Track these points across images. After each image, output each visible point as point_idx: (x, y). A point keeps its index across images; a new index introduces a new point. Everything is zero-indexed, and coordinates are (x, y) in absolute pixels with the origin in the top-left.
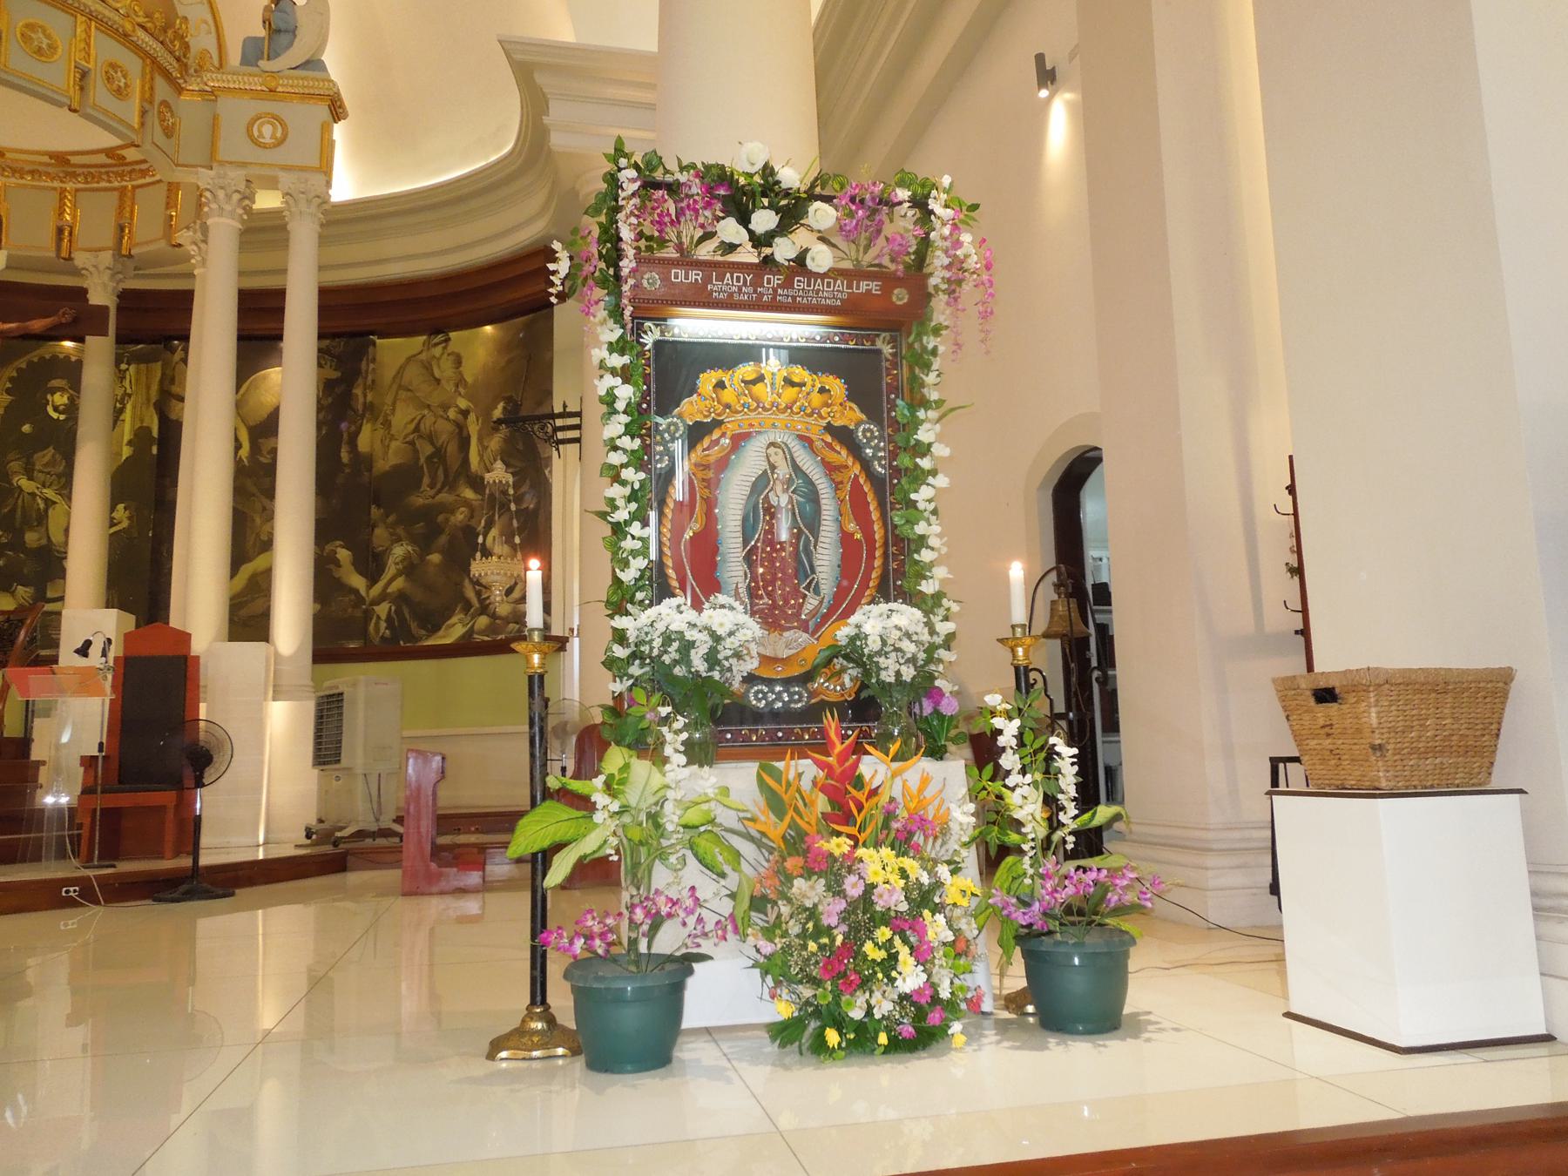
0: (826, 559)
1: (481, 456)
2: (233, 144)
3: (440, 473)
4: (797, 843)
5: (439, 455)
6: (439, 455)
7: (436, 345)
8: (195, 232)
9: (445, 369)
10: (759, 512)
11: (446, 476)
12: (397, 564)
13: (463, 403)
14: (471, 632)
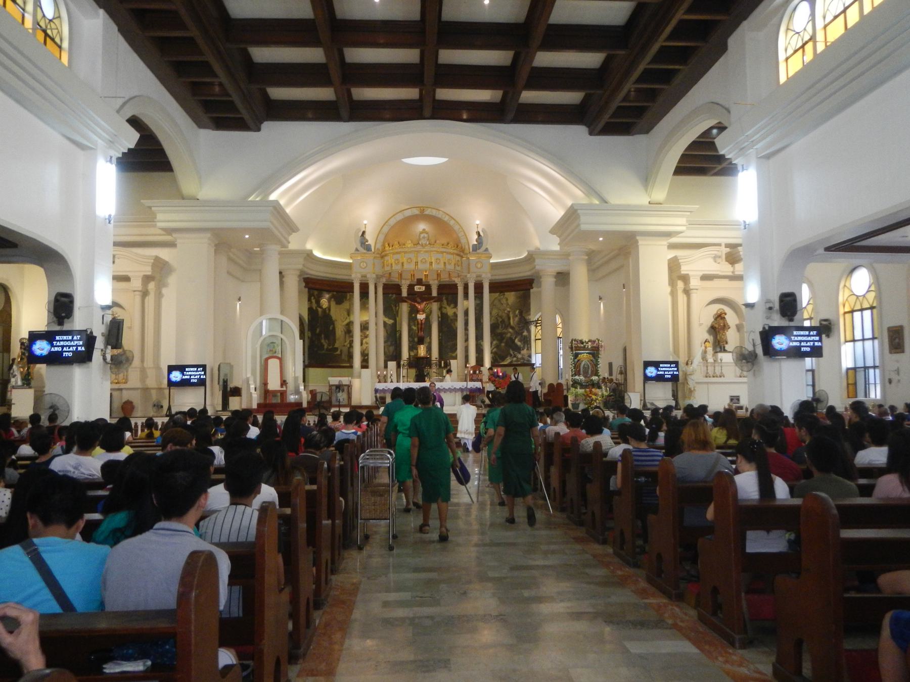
0: (590, 372)
1: (513, 322)
2: (473, 269)
3: (504, 325)
4: (587, 395)
5: (503, 321)
6: (503, 321)
9: (504, 301)
10: (584, 367)
11: (505, 325)
13: (508, 309)
14: (512, 361)
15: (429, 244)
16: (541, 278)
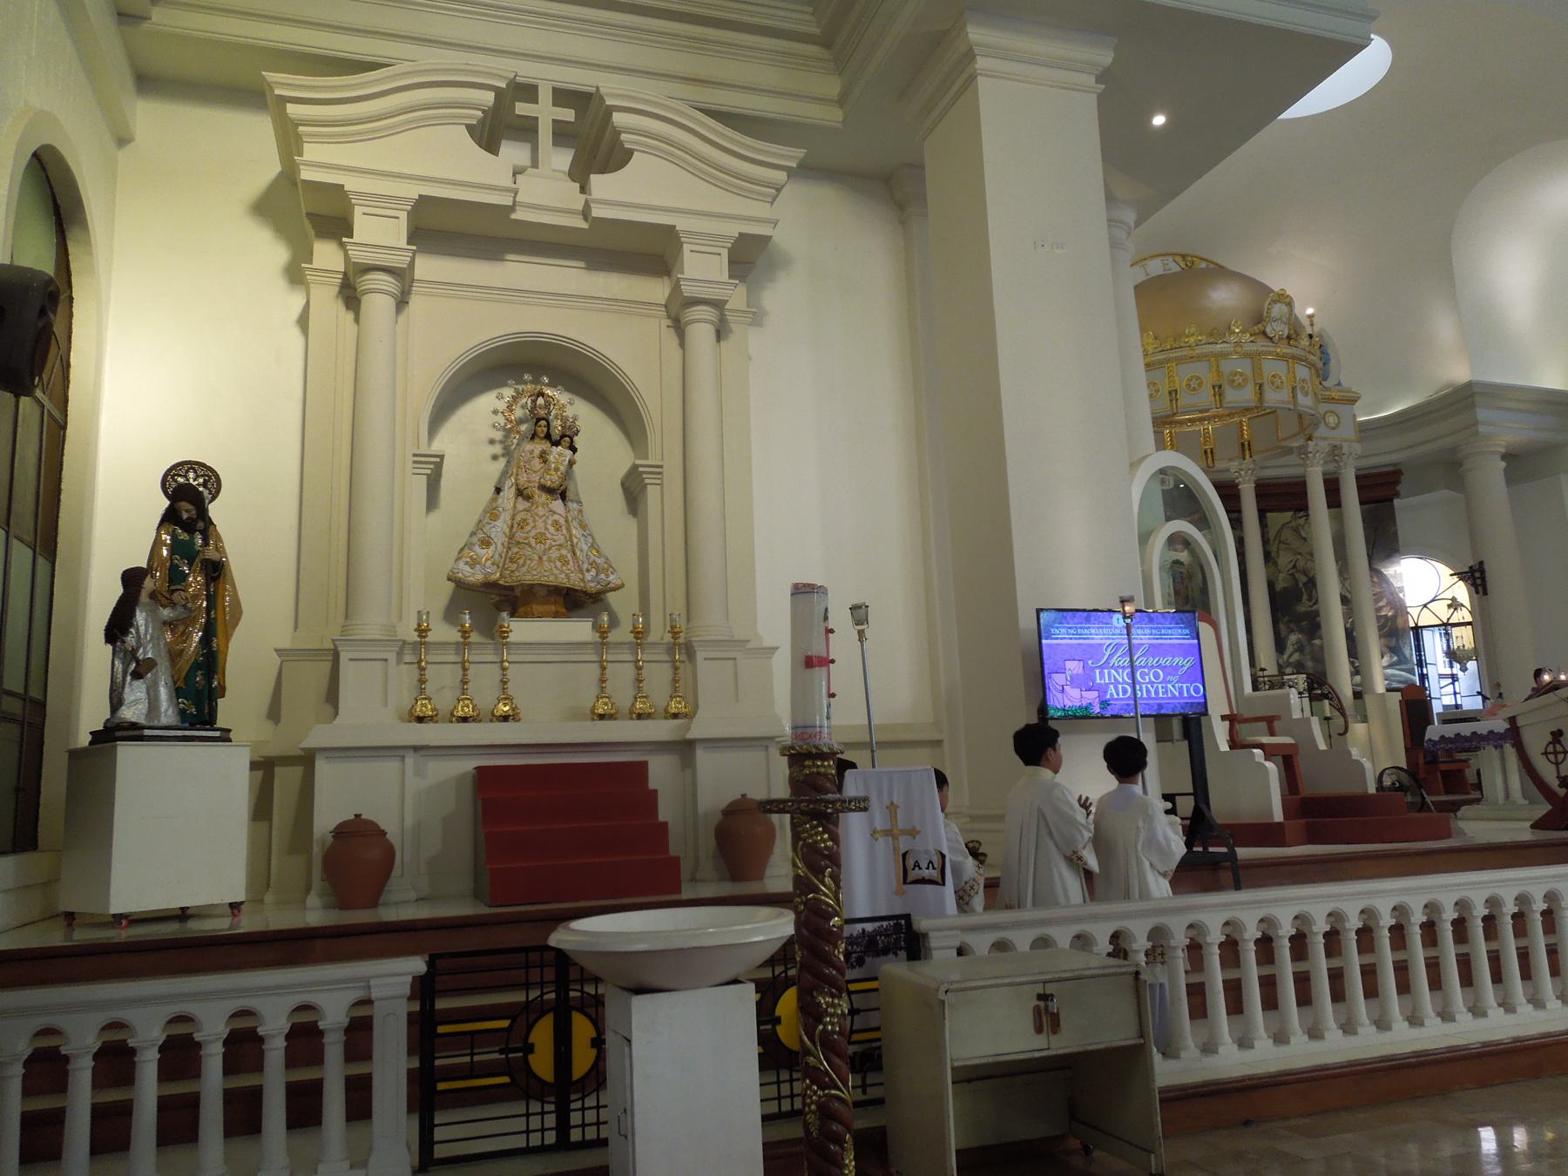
7: (1300, 517)
8: (1241, 464)
12: (1293, 645)
15: (1289, 338)
16: (1461, 465)
